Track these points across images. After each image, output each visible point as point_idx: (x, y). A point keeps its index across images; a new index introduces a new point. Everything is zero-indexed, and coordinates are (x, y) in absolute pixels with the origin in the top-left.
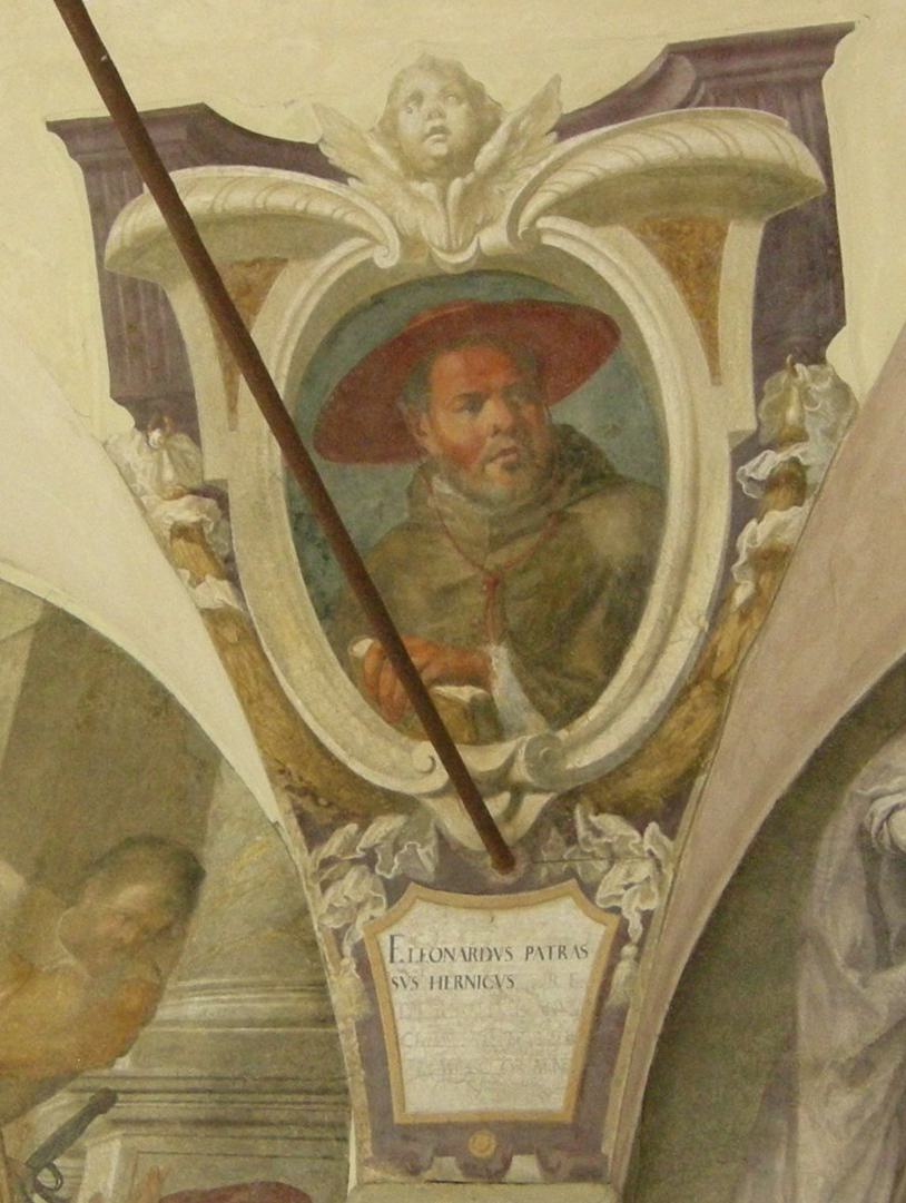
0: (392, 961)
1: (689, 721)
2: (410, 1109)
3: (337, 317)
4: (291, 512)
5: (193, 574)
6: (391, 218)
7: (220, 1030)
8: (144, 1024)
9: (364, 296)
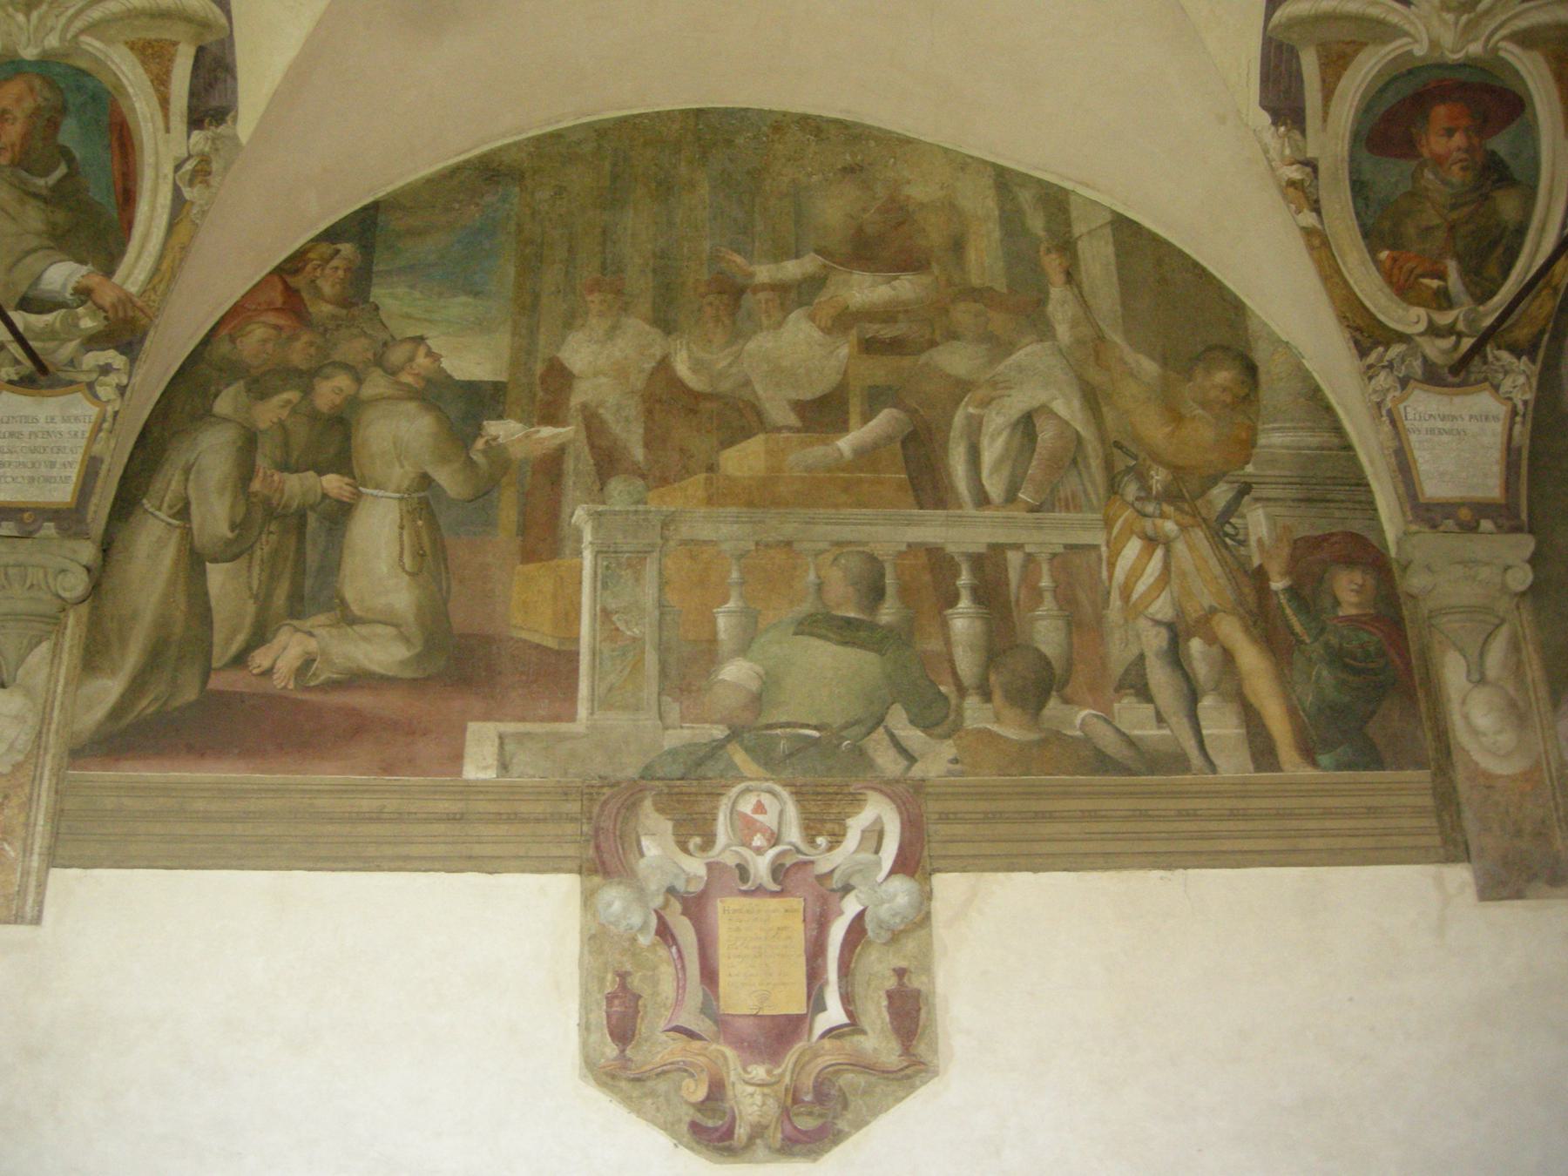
1: (1541, 307)
3: (1387, 78)
4: (1351, 179)
6: (1428, 30)
8: (1253, 447)
9: (1404, 70)
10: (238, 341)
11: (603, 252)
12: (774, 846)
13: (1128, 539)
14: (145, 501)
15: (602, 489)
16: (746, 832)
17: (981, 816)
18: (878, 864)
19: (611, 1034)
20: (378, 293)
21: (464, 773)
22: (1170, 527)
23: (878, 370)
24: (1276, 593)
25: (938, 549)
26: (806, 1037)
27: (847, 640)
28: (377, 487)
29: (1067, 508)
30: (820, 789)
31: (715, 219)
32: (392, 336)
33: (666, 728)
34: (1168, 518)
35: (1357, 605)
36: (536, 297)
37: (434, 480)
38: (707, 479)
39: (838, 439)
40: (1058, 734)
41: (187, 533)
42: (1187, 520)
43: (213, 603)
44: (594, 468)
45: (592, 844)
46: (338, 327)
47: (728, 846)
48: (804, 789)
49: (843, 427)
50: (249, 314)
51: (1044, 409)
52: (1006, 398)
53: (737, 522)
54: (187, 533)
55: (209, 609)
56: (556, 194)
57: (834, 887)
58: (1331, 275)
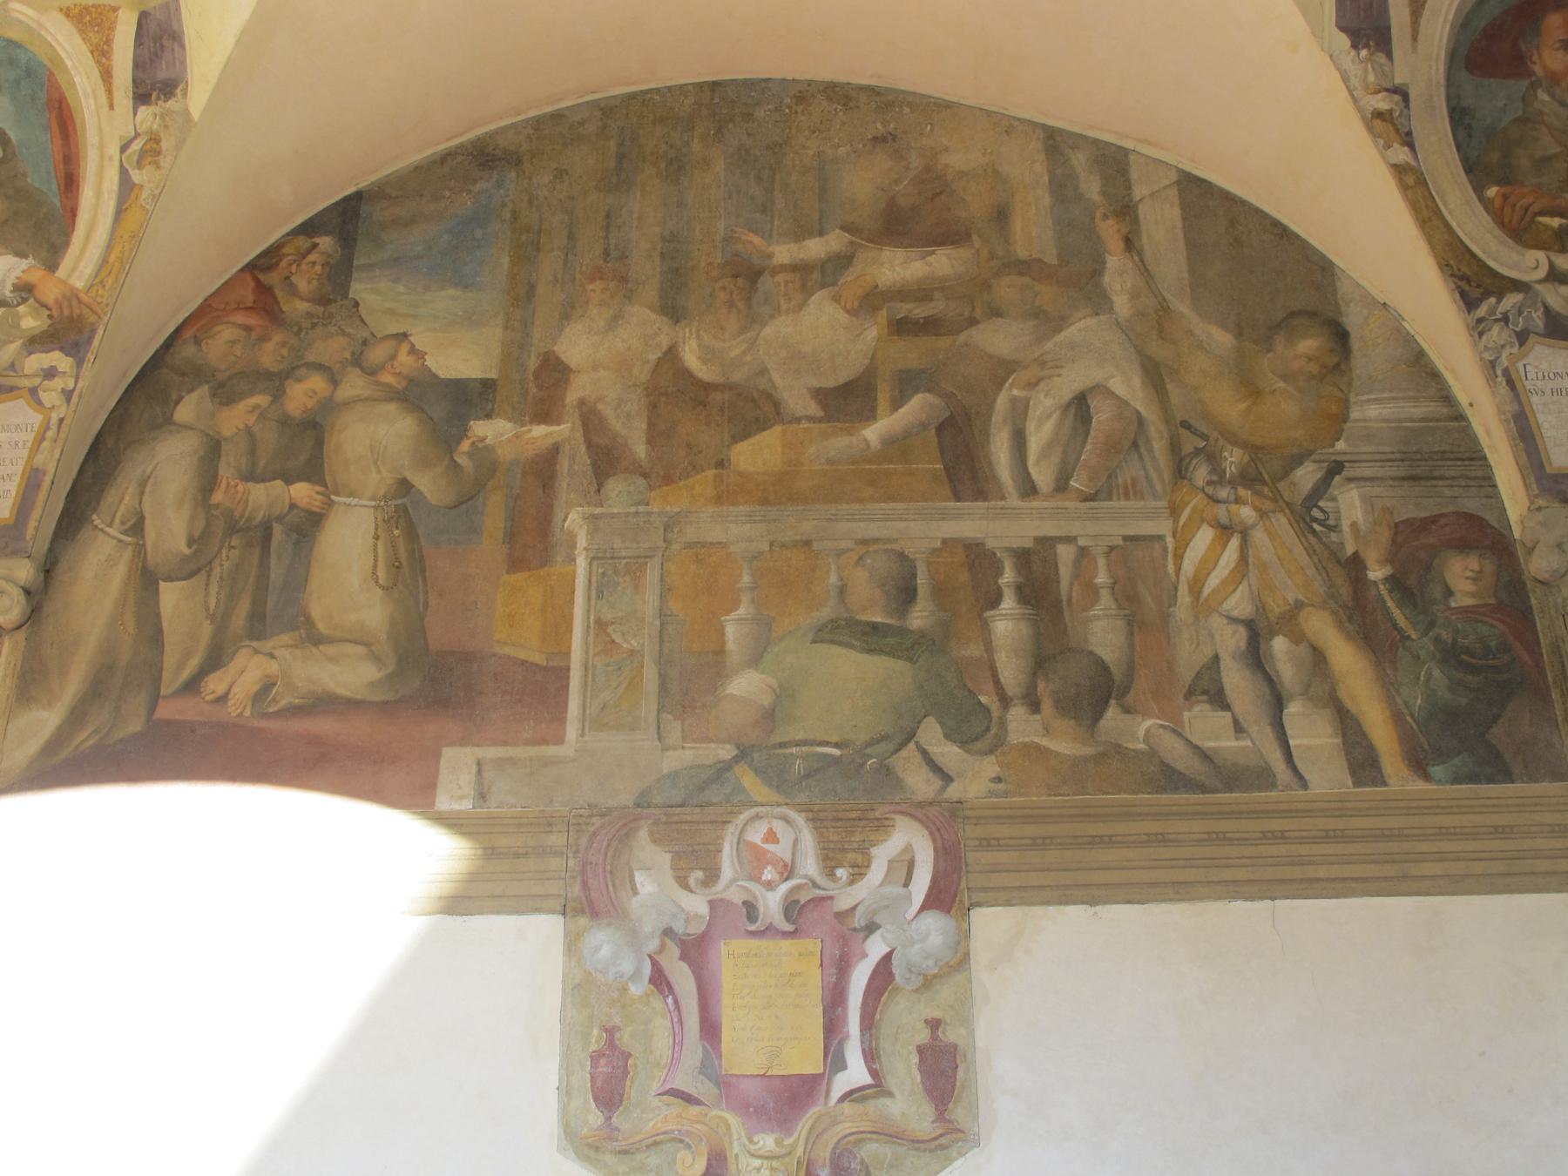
0: (1527, 378)
2: (1555, 465)
4: (1448, 106)
5: (1385, 142)
7: (1393, 425)
10: (203, 345)
11: (606, 237)
12: (786, 880)
13: (1198, 529)
14: (94, 517)
15: (599, 491)
16: (755, 864)
17: (1029, 842)
18: (908, 899)
19: (596, 1099)
20: (359, 289)
21: (437, 804)
22: (1247, 513)
23: (909, 353)
24: (1375, 582)
25: (977, 545)
26: (822, 1099)
27: (872, 648)
28: (352, 494)
29: (1127, 497)
30: (840, 815)
31: (730, 197)
32: (372, 334)
33: (665, 749)
34: (1245, 503)
35: (1473, 595)
36: (532, 288)
37: (413, 486)
38: (716, 476)
39: (865, 428)
40: (1118, 749)
41: (140, 550)
42: (1267, 505)
43: (165, 625)
44: (590, 468)
45: (579, 880)
46: (314, 326)
47: (734, 880)
48: (822, 815)
49: (870, 415)
50: (216, 314)
51: (1100, 389)
52: (1056, 378)
53: (747, 522)
54: (140, 550)
55: (160, 632)
56: (555, 177)
57: (857, 925)
58: (1429, 216)
